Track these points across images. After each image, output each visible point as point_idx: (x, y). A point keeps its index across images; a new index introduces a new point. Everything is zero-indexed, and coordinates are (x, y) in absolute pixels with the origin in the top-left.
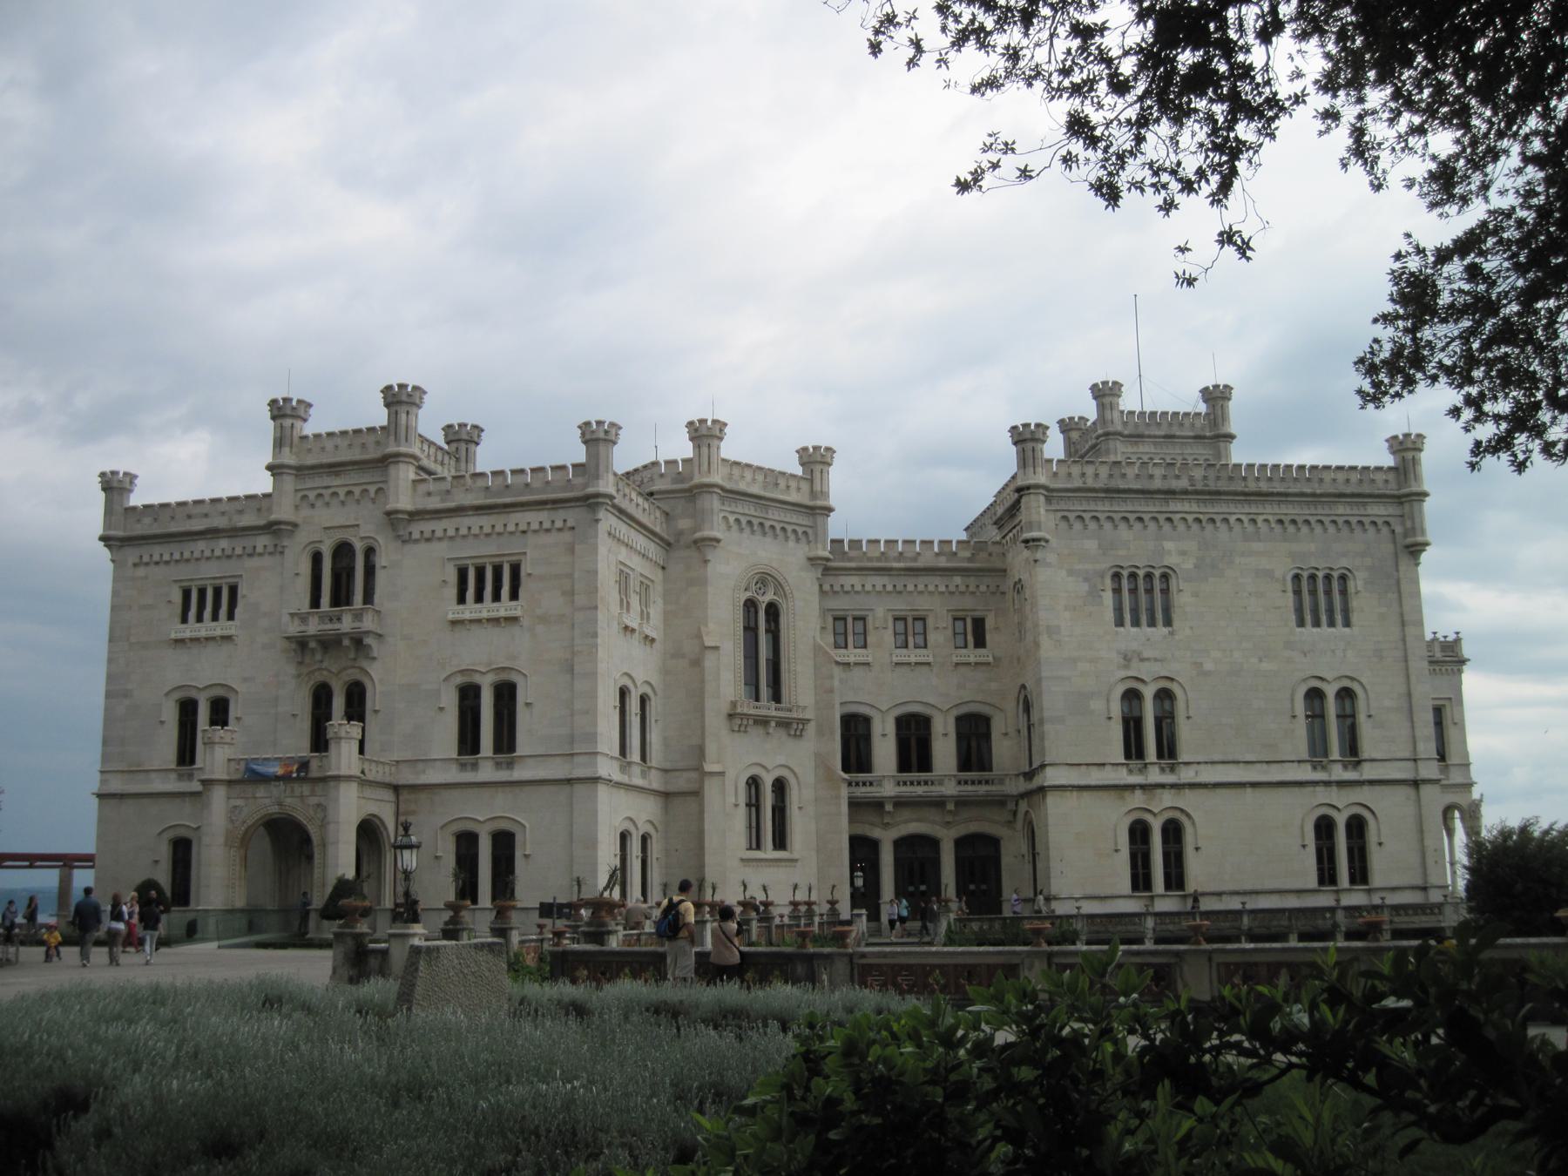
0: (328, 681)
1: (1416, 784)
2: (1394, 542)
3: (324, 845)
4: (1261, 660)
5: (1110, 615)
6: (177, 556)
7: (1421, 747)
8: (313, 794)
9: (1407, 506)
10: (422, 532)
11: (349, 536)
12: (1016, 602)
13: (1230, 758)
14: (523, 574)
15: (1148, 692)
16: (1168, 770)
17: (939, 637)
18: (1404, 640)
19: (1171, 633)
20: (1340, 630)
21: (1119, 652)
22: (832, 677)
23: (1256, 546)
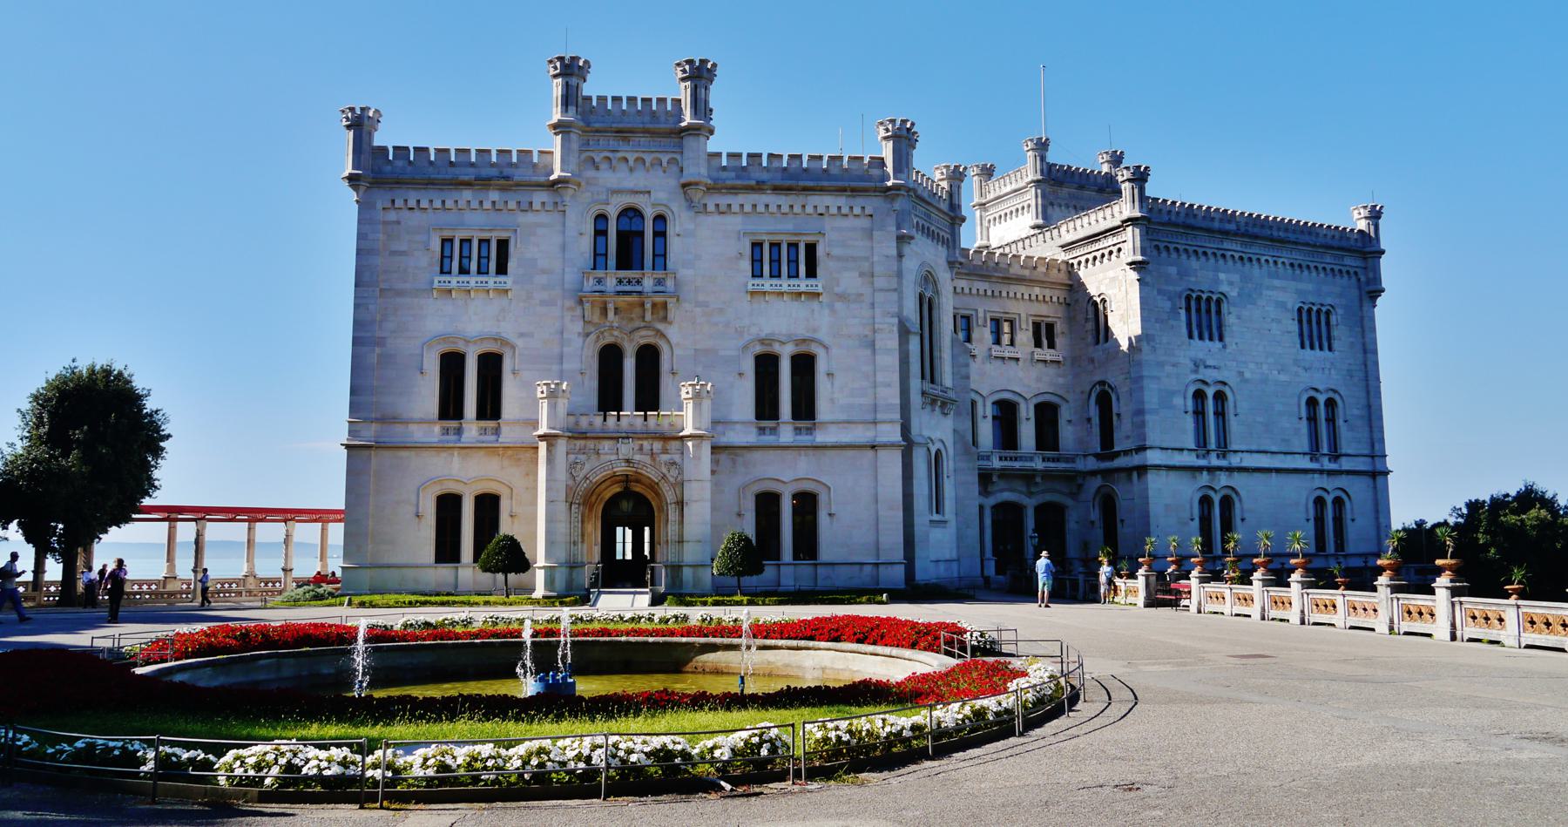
0: (619, 341)
2: (1360, 288)
3: (681, 504)
4: (1279, 373)
5: (1184, 331)
6: (437, 204)
7: (1377, 447)
8: (665, 451)
9: (1370, 260)
10: (717, 205)
11: (639, 201)
12: (1090, 313)
13: (1262, 448)
14: (820, 251)
15: (1210, 392)
16: (1221, 456)
17: (1025, 337)
18: (1366, 365)
19: (1224, 347)
20: (1326, 352)
21: (1191, 360)
22: (967, 365)
23: (1277, 283)
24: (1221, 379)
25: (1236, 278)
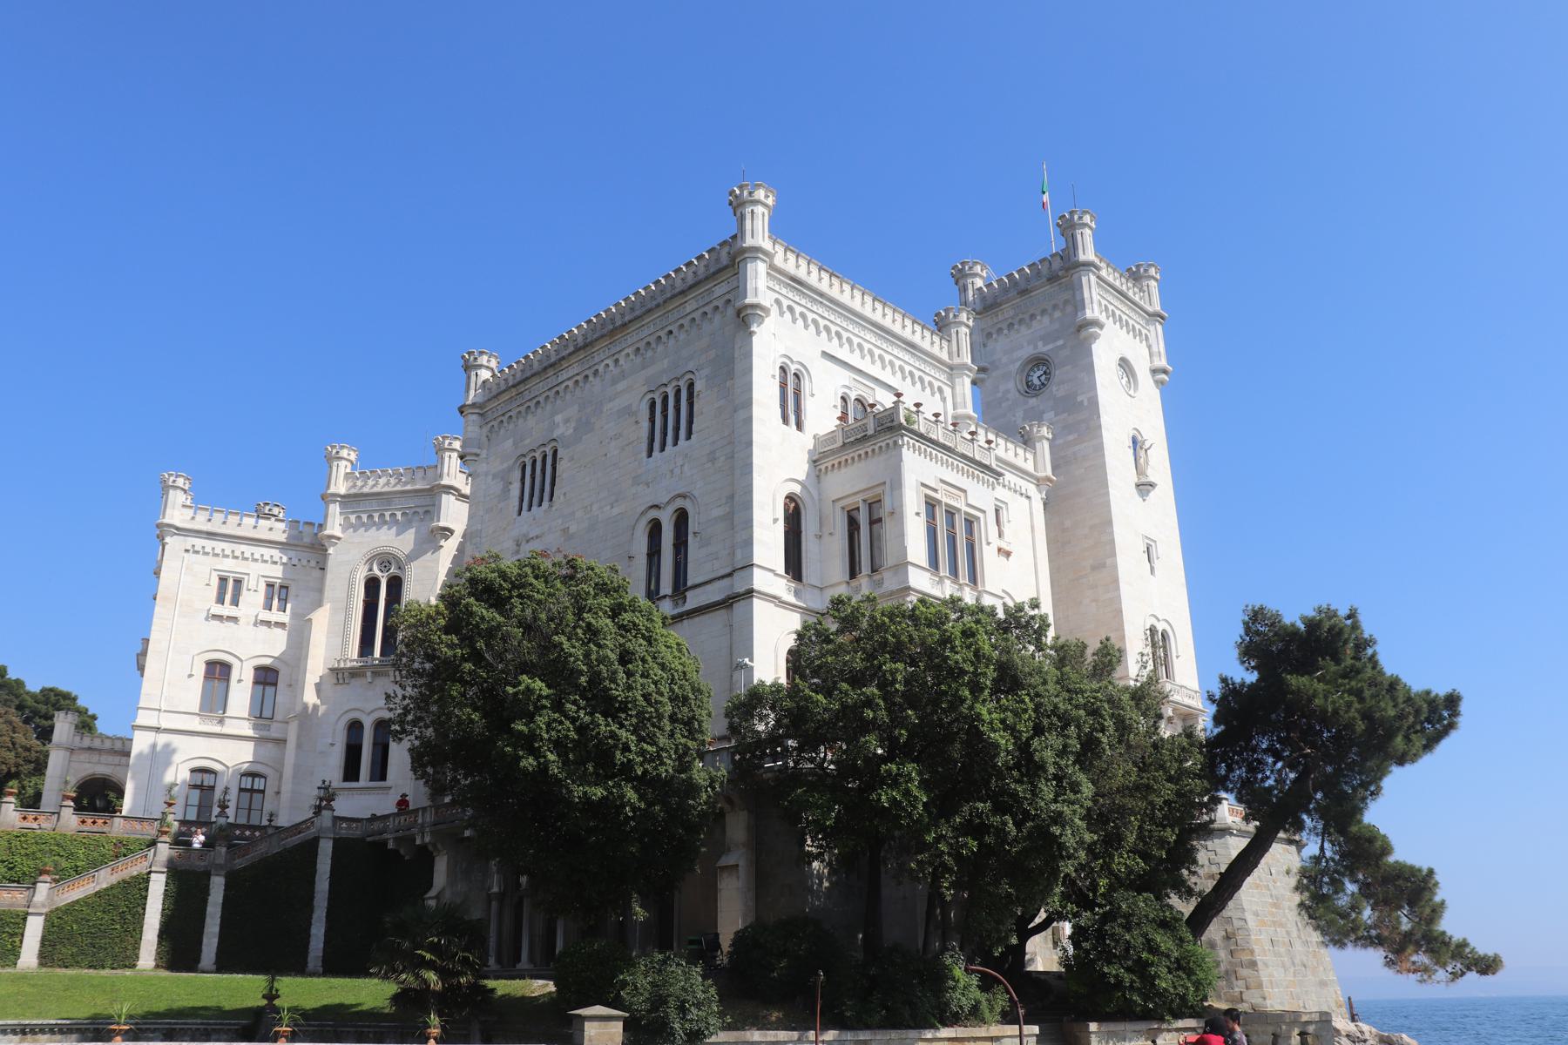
1: (728, 603)
19: (551, 506)
23: (621, 386)
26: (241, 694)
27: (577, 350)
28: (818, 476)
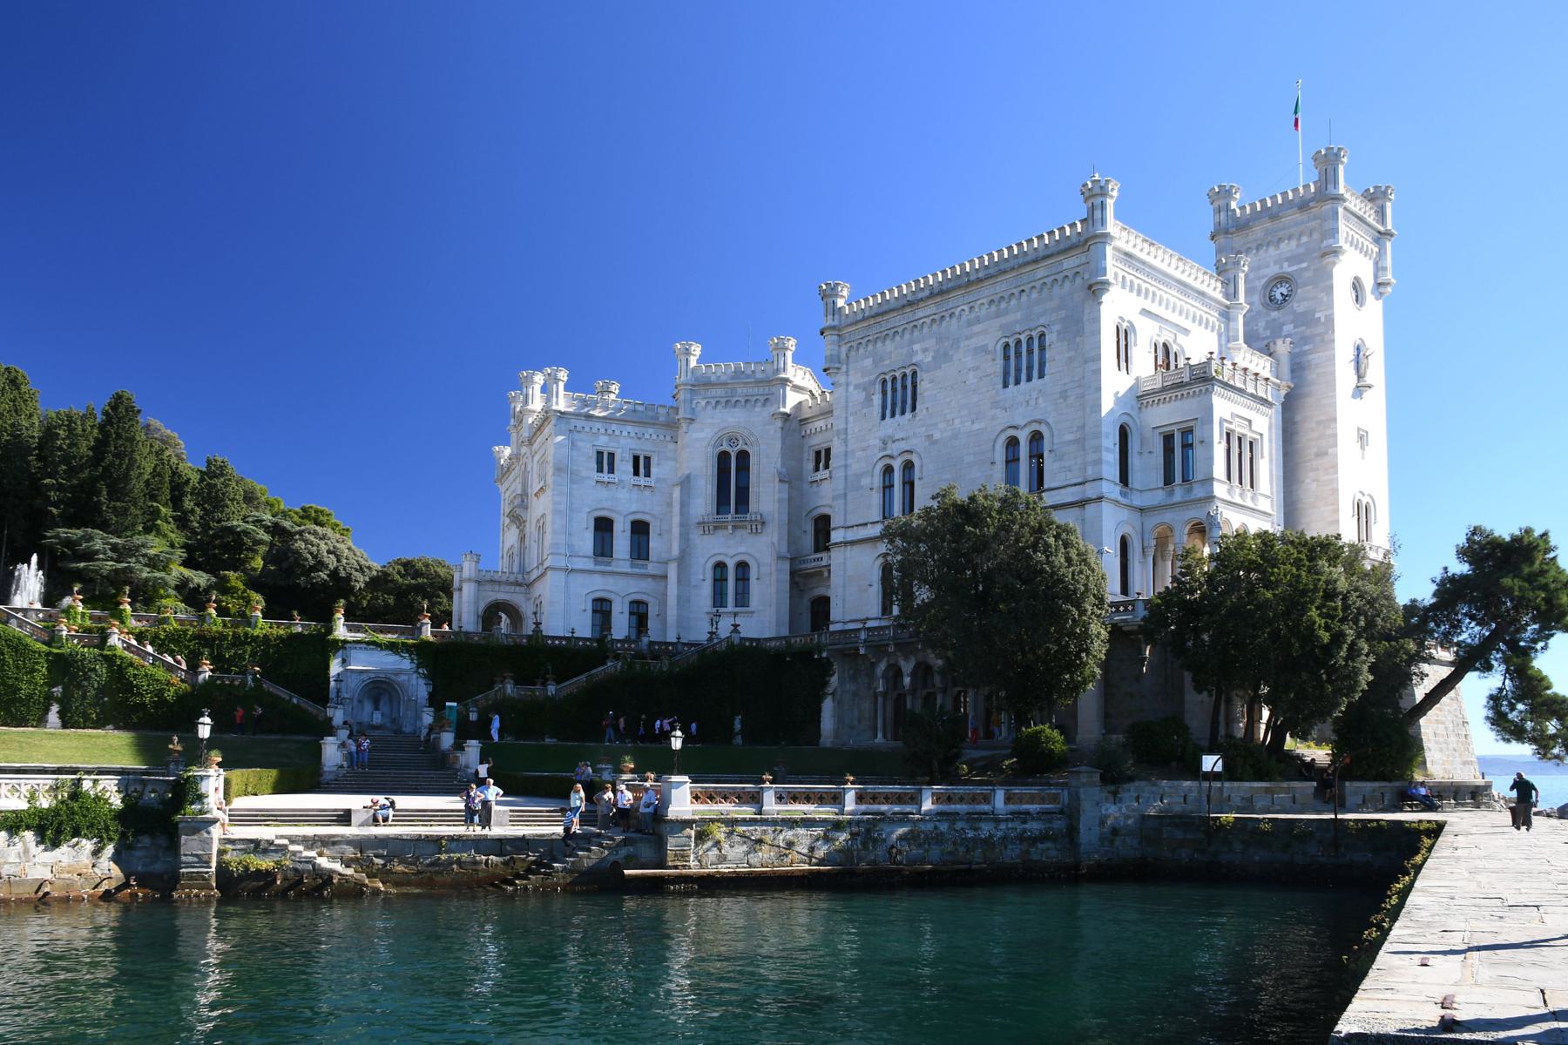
1: (1082, 504)
4: (973, 423)
7: (1090, 470)
19: (914, 417)
24: (908, 448)
25: (931, 343)
26: (622, 541)
27: (932, 295)
28: (1140, 408)
